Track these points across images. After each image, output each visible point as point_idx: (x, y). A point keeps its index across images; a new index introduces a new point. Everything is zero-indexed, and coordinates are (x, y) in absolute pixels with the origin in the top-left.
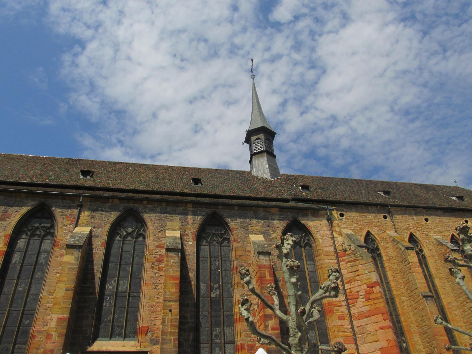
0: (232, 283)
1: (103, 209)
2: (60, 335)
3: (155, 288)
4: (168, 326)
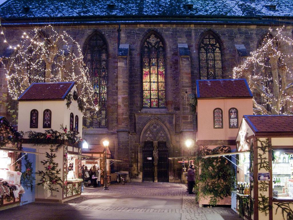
1: (134, 32)
2: (125, 105)
4: (185, 100)
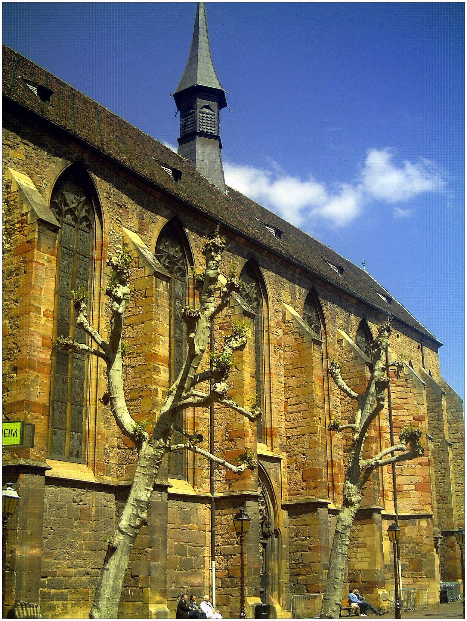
3: (279, 381)
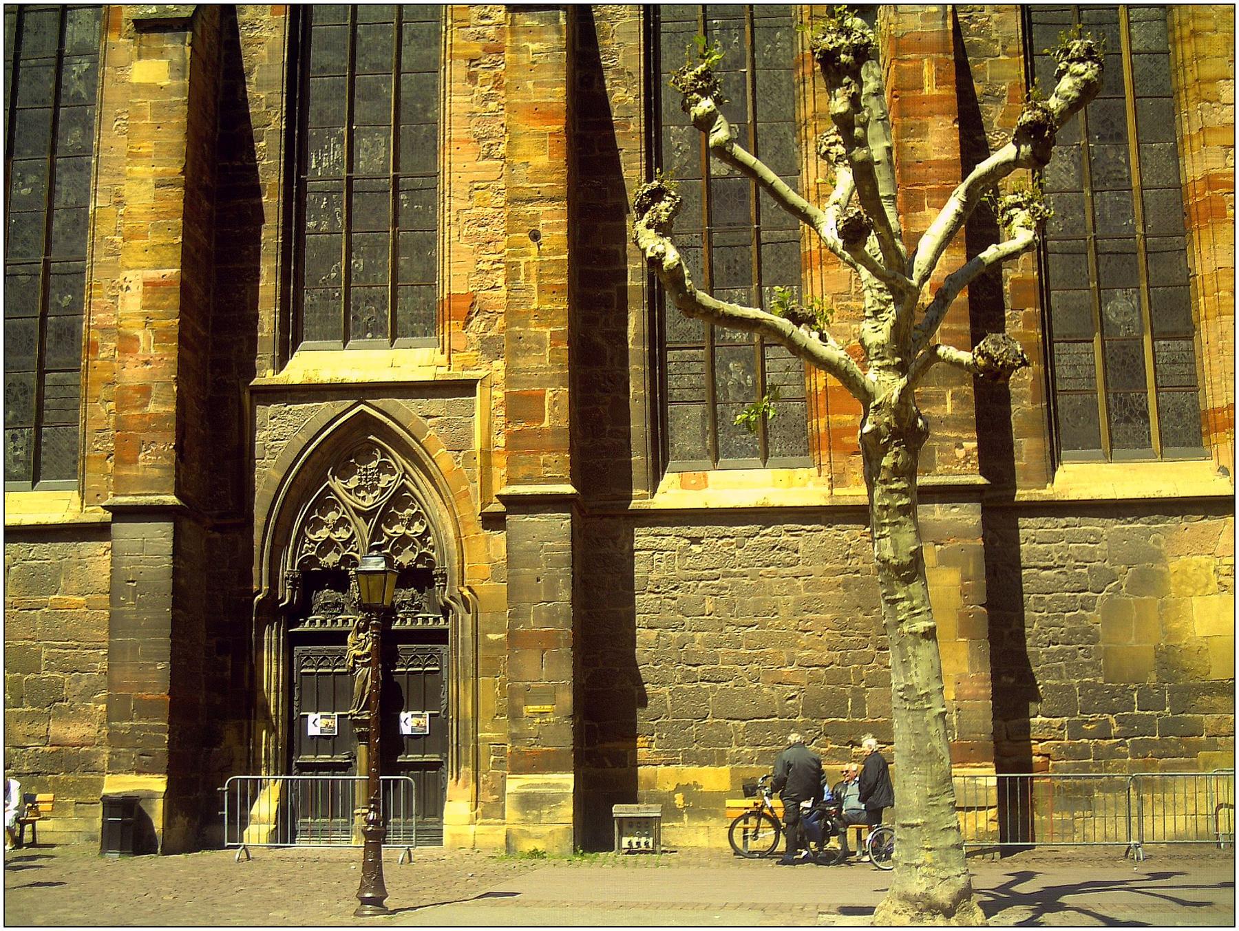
0: (797, 119)
2: (161, 337)
3: (488, 156)
4: (528, 289)
